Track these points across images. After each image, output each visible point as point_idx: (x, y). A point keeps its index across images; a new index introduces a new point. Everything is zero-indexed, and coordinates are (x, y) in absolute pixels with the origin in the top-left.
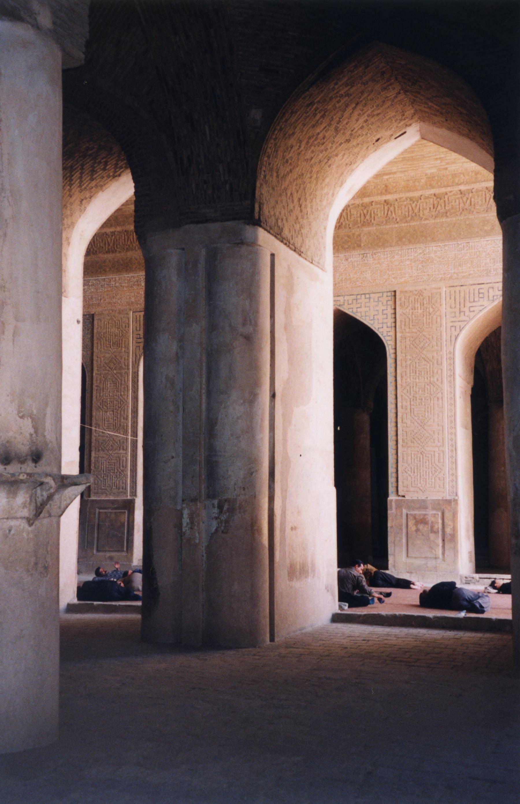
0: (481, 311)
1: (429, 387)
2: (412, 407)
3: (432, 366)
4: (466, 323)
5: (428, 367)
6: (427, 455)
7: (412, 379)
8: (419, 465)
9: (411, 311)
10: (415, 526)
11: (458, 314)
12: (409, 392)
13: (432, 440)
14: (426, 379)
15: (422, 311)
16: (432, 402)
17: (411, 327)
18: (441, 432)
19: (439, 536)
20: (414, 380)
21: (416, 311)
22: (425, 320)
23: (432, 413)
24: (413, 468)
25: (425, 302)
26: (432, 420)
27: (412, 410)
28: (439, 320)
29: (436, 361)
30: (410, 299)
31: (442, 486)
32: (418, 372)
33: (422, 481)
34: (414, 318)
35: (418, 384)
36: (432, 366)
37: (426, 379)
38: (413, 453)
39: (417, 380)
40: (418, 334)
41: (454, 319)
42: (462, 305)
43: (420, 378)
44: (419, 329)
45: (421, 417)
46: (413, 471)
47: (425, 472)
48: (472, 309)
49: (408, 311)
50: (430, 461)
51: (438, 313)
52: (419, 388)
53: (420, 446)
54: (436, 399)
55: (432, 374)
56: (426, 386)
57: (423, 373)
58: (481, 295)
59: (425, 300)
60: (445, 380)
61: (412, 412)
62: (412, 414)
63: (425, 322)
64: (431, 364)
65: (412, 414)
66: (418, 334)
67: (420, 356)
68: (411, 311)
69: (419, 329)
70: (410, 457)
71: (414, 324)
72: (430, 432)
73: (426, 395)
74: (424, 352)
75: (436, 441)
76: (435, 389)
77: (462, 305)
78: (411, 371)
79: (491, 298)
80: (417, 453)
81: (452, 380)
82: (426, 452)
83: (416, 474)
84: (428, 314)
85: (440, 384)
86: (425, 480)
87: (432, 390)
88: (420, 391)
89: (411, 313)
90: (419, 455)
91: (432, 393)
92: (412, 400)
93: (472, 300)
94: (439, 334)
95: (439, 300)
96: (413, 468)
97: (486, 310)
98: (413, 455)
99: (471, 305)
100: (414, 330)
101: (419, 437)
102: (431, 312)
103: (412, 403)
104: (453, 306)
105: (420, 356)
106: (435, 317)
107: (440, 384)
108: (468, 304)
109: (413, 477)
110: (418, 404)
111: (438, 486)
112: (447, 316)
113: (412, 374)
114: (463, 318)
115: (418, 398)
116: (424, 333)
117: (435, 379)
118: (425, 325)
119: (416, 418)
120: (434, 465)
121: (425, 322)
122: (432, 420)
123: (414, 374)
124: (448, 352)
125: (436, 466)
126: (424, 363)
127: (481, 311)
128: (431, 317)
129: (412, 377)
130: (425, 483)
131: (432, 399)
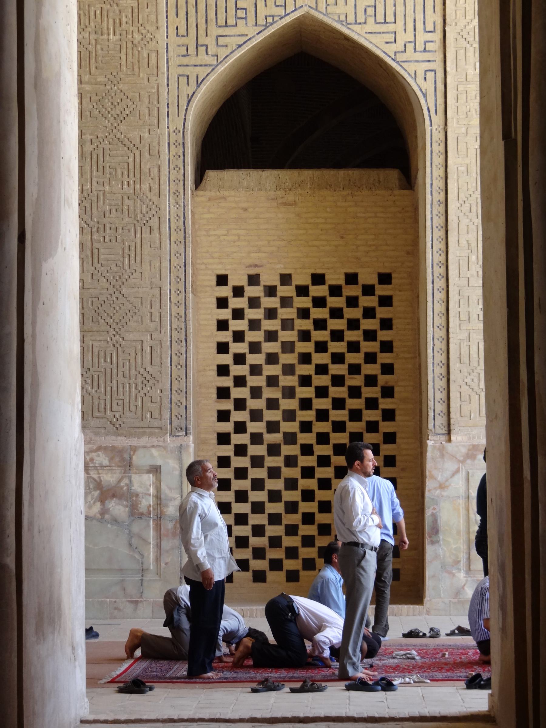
0: (240, 46)
1: (132, 204)
2: (96, 245)
3: (138, 160)
4: (209, 69)
5: (131, 159)
6: (127, 350)
7: (95, 184)
8: (108, 371)
9: (93, 36)
10: (98, 504)
11: (192, 50)
12: (89, 213)
13: (137, 318)
14: (125, 187)
15: (118, 37)
16: (138, 235)
17: (93, 70)
18: (158, 300)
19: (148, 526)
20: (101, 188)
21: (105, 37)
22: (124, 58)
23: (138, 259)
24: (96, 377)
25: (124, 20)
26: (137, 275)
27: (95, 251)
28: (153, 61)
29: (147, 147)
30: (92, 9)
31: (158, 416)
32: (107, 170)
33: (114, 405)
34: (100, 52)
35: (108, 196)
36: (138, 160)
37: (125, 187)
38: (96, 344)
39: (107, 188)
40: (108, 87)
41: (185, 61)
42: (202, 32)
43: (113, 182)
44: (112, 77)
45: (114, 268)
46: (95, 384)
47: (121, 386)
48: (221, 41)
49: (87, 36)
50: (133, 361)
51: (152, 45)
52: (110, 205)
53: (112, 332)
54: (146, 230)
55: (138, 175)
56: (126, 201)
57: (119, 172)
58: (241, 14)
59: (123, 15)
60: (165, 188)
61: (95, 256)
62: (96, 261)
63: (124, 63)
64: (137, 153)
65: (96, 261)
66: (108, 87)
67: (112, 136)
68: (93, 36)
69: (112, 77)
70: (90, 354)
71: (100, 64)
72: (133, 299)
73: (126, 219)
74: (122, 127)
75: (147, 319)
76: (144, 207)
77: (202, 32)
78: (94, 168)
79: (261, 21)
80: (104, 344)
81: (181, 191)
82: (123, 343)
83: (102, 389)
84: (130, 45)
85: (155, 199)
86: (120, 402)
87: (138, 211)
88: (114, 211)
89: (93, 42)
90: (111, 349)
91: (139, 216)
92: (95, 230)
93: (222, 22)
94: (154, 90)
95: (153, 17)
96: (96, 377)
97: (250, 45)
98: (96, 350)
99: (221, 31)
100: (101, 79)
101: (111, 311)
102: (136, 42)
103: (95, 237)
104: (182, 31)
105: (112, 136)
106: (145, 54)
107: (155, 199)
108: (214, 31)
109: (96, 396)
110: (107, 240)
111: (148, 416)
112: (171, 54)
113: (95, 173)
114: (203, 58)
115: (108, 226)
116: (121, 86)
117: (145, 187)
118: (124, 68)
119: (104, 270)
120: (142, 371)
121: (124, 63)
122: (137, 275)
123: (100, 174)
124: (171, 130)
125: (145, 374)
126: (122, 150)
127: (240, 46)
128: (136, 52)
129: (95, 180)
130: (120, 408)
131: (138, 229)
